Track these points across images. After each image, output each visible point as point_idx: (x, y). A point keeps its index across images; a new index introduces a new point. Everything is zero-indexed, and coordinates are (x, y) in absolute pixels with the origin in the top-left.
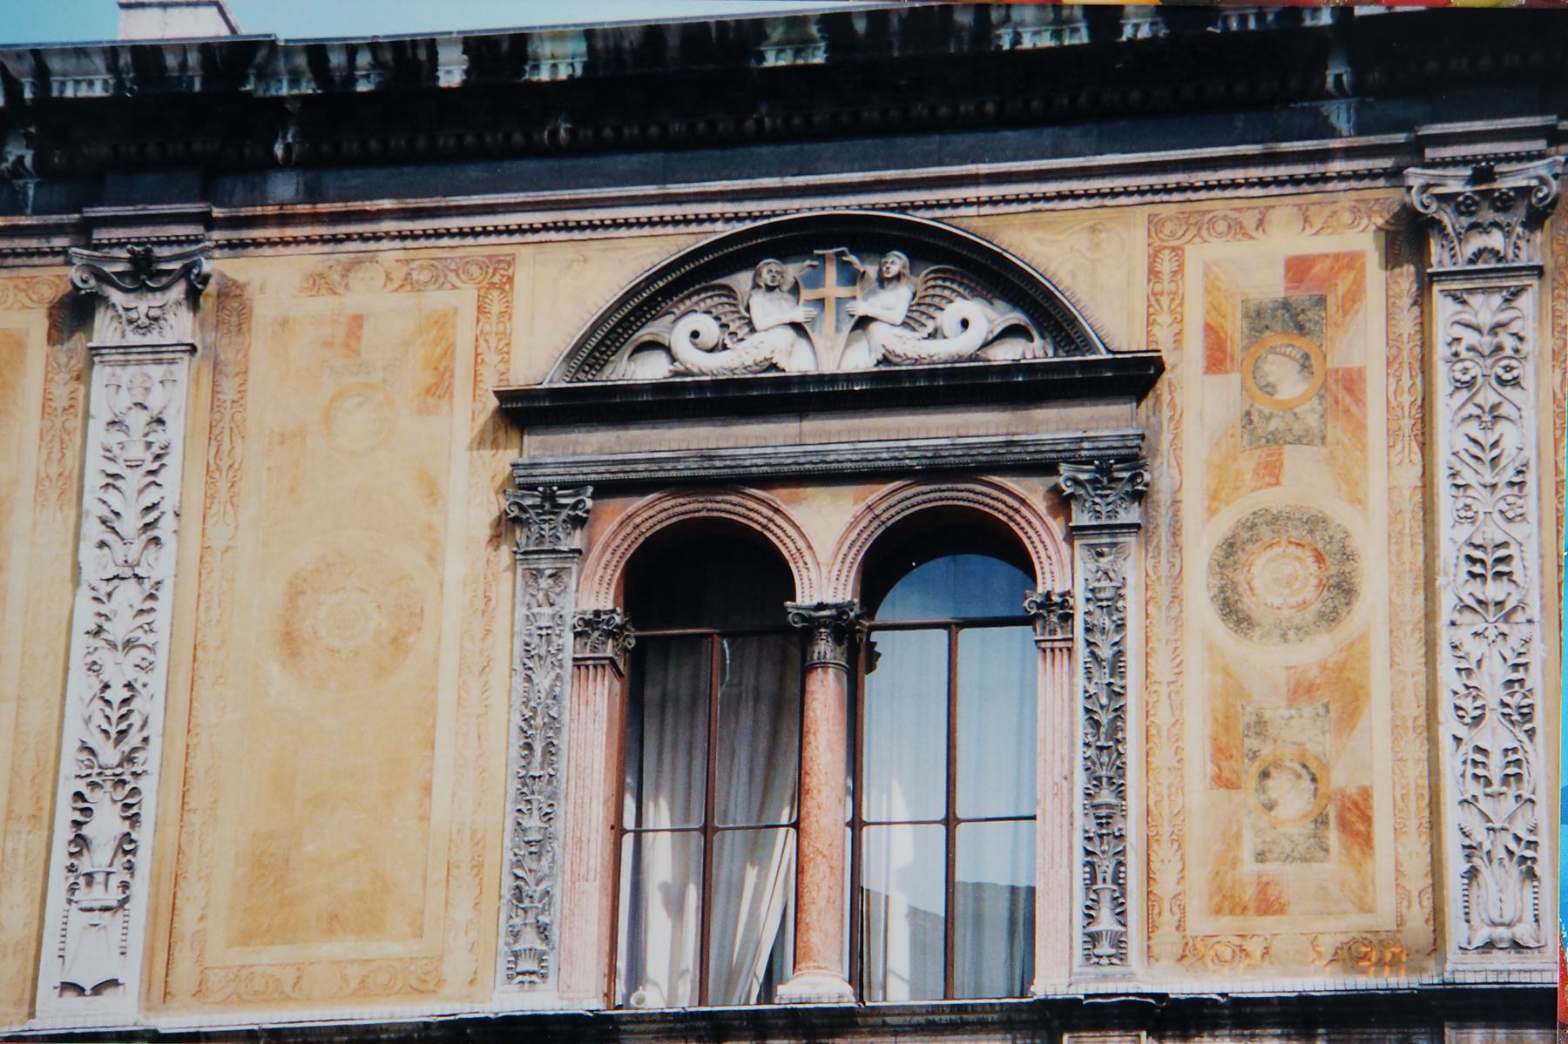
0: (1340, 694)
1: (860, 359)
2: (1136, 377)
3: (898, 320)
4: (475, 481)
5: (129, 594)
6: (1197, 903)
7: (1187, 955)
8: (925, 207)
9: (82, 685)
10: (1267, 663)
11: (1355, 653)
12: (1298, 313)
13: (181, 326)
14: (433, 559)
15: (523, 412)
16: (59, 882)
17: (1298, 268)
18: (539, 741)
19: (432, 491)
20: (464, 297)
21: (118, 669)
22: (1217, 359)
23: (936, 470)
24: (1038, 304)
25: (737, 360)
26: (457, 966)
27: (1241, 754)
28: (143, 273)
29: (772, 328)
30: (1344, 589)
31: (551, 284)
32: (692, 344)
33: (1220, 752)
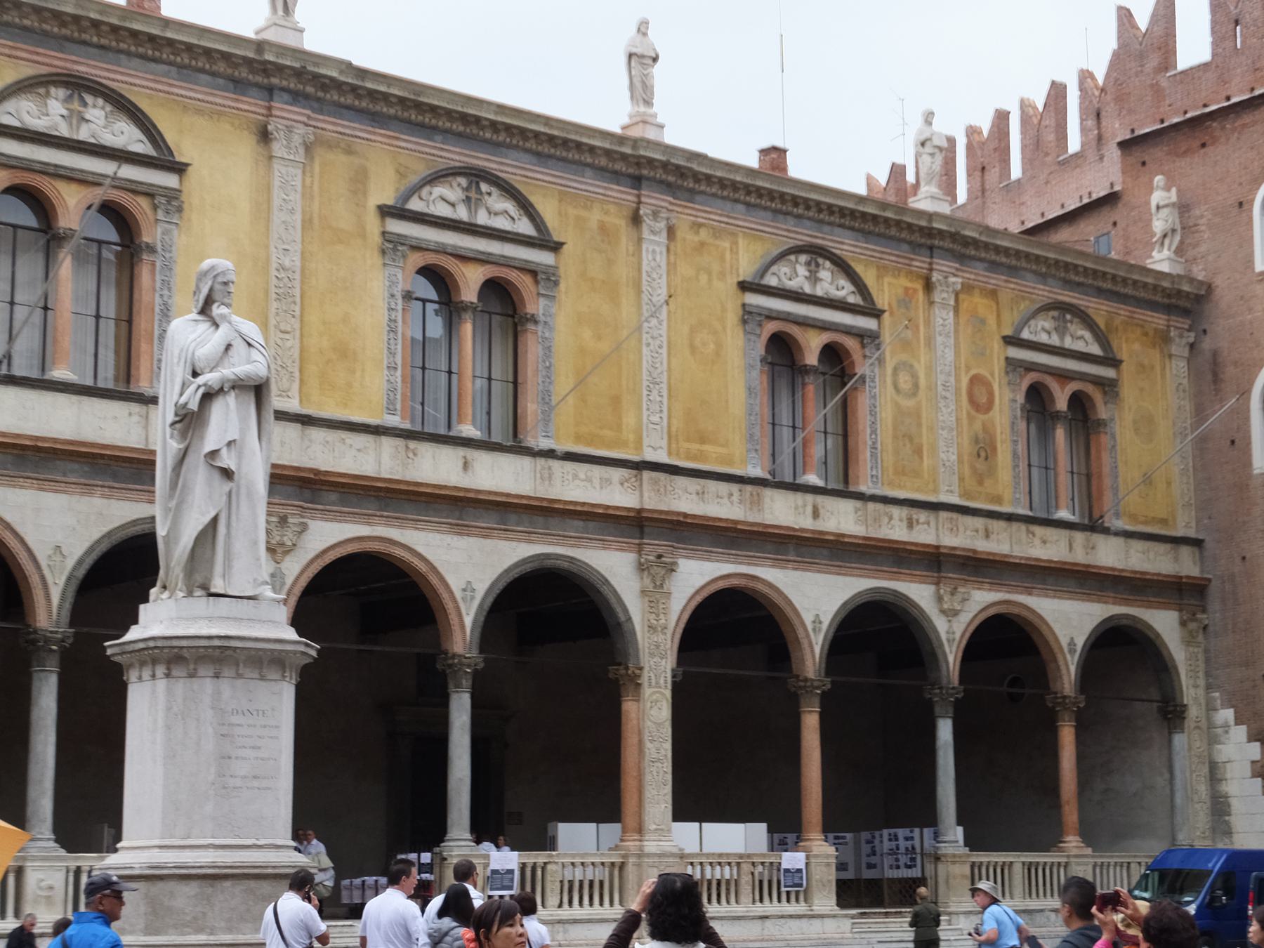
1: (819, 292)
6: (891, 470)
14: (724, 328)
15: (744, 286)
17: (907, 289)
19: (724, 310)
20: (727, 245)
24: (861, 287)
29: (794, 275)
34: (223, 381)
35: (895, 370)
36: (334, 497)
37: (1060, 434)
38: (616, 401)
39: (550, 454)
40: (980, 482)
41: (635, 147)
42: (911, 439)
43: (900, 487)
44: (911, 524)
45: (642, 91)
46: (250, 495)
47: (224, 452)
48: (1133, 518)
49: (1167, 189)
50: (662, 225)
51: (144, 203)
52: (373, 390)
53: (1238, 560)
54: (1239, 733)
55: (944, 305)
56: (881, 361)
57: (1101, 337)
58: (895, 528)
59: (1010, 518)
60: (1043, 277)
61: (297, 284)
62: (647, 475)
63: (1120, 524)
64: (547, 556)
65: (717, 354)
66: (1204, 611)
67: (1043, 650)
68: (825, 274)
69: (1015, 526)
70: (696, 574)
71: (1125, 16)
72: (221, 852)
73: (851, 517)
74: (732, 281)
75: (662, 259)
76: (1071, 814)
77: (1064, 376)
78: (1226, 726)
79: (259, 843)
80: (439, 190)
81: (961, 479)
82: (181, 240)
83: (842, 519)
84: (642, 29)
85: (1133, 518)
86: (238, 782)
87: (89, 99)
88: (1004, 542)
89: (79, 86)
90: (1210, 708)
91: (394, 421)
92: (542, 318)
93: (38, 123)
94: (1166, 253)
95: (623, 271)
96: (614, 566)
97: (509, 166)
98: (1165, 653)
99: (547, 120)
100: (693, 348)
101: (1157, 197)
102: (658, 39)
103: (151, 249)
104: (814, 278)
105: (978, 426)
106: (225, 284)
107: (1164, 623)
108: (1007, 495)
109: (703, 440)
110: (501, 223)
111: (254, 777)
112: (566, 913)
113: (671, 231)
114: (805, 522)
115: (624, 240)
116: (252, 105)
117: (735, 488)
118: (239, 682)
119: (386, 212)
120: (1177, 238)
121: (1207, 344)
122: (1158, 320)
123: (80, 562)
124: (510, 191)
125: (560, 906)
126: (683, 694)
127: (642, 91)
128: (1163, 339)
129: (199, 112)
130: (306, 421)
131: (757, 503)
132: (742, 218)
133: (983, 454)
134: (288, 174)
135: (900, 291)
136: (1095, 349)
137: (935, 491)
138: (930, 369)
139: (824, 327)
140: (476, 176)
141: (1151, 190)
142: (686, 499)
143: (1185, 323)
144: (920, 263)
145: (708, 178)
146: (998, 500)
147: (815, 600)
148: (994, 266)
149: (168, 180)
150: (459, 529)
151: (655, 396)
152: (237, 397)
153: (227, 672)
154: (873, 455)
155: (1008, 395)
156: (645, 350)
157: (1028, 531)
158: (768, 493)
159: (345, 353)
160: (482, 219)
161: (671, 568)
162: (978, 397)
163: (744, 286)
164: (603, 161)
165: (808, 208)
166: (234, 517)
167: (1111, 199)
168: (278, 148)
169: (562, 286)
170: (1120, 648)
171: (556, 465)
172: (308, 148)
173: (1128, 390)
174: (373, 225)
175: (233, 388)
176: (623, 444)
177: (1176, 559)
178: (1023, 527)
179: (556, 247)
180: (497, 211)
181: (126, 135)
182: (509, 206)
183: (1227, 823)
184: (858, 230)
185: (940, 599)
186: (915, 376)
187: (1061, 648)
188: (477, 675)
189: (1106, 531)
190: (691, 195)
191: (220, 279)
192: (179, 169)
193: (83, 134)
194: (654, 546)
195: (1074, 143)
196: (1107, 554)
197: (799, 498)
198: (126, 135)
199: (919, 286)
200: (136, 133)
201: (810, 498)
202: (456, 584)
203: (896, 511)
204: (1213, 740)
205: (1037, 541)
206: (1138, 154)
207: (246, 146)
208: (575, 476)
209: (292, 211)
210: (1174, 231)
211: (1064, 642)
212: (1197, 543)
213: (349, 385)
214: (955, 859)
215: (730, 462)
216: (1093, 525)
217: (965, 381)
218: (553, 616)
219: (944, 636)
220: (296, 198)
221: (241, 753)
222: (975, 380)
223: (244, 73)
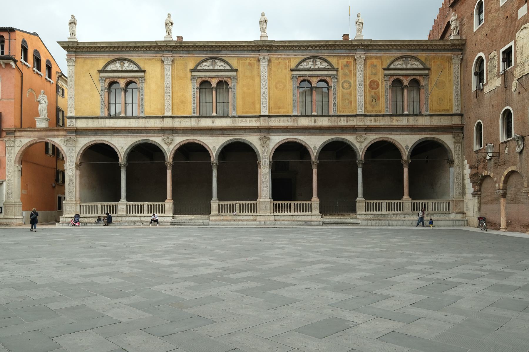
0: (350, 94)
2: (337, 70)
3: (319, 64)
4: (289, 75)
7: (340, 112)
10: (345, 91)
11: (351, 90)
12: (347, 65)
15: (292, 70)
17: (347, 62)
19: (286, 76)
20: (287, 61)
22: (342, 69)
25: (308, 67)
29: (310, 64)
30: (350, 86)
32: (303, 66)
33: (342, 97)
35: (343, 83)
36: (181, 132)
38: (254, 103)
39: (234, 117)
41: (254, 43)
42: (348, 100)
44: (347, 121)
45: (263, 30)
49: (455, 15)
50: (266, 60)
51: (137, 79)
52: (190, 109)
55: (360, 63)
56: (338, 81)
57: (421, 62)
58: (343, 122)
59: (383, 116)
60: (400, 50)
62: (261, 118)
63: (428, 113)
64: (235, 139)
65: (284, 87)
66: (463, 133)
69: (385, 118)
70: (277, 140)
73: (327, 121)
74: (288, 69)
75: (266, 68)
76: (406, 190)
77: (406, 76)
80: (204, 64)
82: (145, 86)
83: (324, 122)
84: (263, 14)
85: (435, 111)
88: (381, 122)
89: (122, 60)
91: (195, 115)
93: (115, 69)
95: (255, 73)
96: (254, 140)
98: (446, 146)
99: (229, 42)
100: (276, 88)
104: (315, 64)
105: (373, 93)
107: (447, 139)
109: (279, 108)
113: (269, 61)
115: (256, 65)
116: (159, 55)
117: (289, 118)
119: (192, 71)
122: (449, 54)
123: (127, 150)
127: (263, 30)
128: (449, 60)
129: (148, 59)
130: (173, 117)
131: (296, 121)
132: (291, 53)
133: (374, 100)
135: (345, 63)
136: (421, 66)
137: (356, 112)
138: (355, 81)
139: (318, 76)
140: (214, 59)
142: (274, 123)
143: (460, 53)
144: (351, 54)
145: (278, 46)
146: (380, 111)
148: (380, 50)
149: (142, 74)
150: (211, 136)
151: (264, 100)
154: (334, 106)
155: (384, 83)
156: (261, 90)
157: (391, 118)
158: (300, 118)
159: (183, 102)
160: (216, 68)
161: (269, 139)
162: (373, 85)
163: (292, 70)
164: (249, 48)
165: (320, 47)
168: (165, 63)
169: (239, 79)
171: (236, 119)
172: (173, 61)
174: (189, 74)
176: (256, 112)
177: (452, 120)
178: (389, 118)
179: (236, 71)
180: (220, 65)
181: (132, 67)
182: (223, 64)
184: (330, 50)
187: (403, 148)
189: (422, 115)
190: (276, 51)
192: (144, 71)
193: (124, 69)
194: (263, 135)
196: (423, 121)
197: (310, 118)
198: (132, 67)
199: (352, 60)
200: (135, 66)
201: (313, 118)
203: (342, 118)
205: (394, 121)
207: (159, 64)
208: (242, 121)
210: (457, 27)
211: (404, 146)
212: (461, 115)
213: (184, 109)
219: (358, 148)
223: (157, 49)
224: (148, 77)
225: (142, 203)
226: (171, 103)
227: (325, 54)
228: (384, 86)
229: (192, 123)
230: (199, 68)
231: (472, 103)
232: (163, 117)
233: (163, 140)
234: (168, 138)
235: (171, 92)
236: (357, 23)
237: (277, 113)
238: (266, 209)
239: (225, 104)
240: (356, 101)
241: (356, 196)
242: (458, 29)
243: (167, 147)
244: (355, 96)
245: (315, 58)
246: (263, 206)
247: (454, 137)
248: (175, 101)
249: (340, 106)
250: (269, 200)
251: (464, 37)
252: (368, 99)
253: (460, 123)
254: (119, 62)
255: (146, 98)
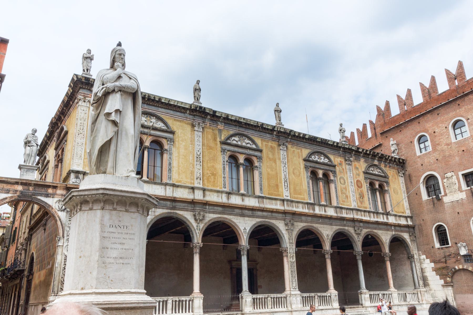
0: (345, 188)
2: (334, 166)
3: (323, 160)
5: (285, 168)
7: (341, 204)
8: (325, 152)
9: (283, 174)
13: (285, 149)
16: (284, 188)
17: (340, 161)
18: (308, 184)
20: (300, 151)
21: (285, 173)
23: (326, 170)
24: (330, 160)
26: (306, 198)
27: (342, 193)
28: (283, 144)
29: (315, 158)
30: (345, 182)
31: (305, 152)
32: (313, 158)
34: (115, 87)
35: (340, 178)
37: (378, 193)
38: (277, 186)
40: (362, 204)
43: (343, 205)
46: (127, 134)
47: (113, 114)
48: (396, 212)
51: (164, 140)
53: (422, 221)
54: (428, 261)
61: (201, 158)
67: (380, 243)
68: (323, 158)
71: (378, 109)
72: (99, 296)
78: (424, 259)
79: (122, 291)
80: (233, 138)
81: (357, 203)
86: (112, 260)
87: (152, 117)
90: (419, 255)
91: (226, 190)
92: (258, 166)
94: (395, 154)
95: (277, 156)
97: (249, 133)
100: (294, 173)
101: (392, 142)
102: (281, 107)
103: (166, 150)
105: (359, 191)
106: (120, 54)
107: (406, 236)
108: (368, 206)
110: (248, 145)
111: (121, 258)
112: (273, 310)
114: (323, 213)
118: (114, 212)
120: (397, 151)
121: (407, 173)
124: (250, 139)
125: (272, 308)
126: (298, 254)
127: (279, 119)
134: (198, 135)
135: (339, 162)
141: (389, 141)
146: (366, 208)
147: (327, 233)
149: (170, 136)
152: (121, 95)
153: (107, 207)
156: (283, 174)
159: (214, 175)
160: (244, 144)
166: (119, 144)
167: (380, 145)
168: (196, 128)
169: (263, 159)
170: (397, 242)
172: (203, 128)
173: (391, 184)
175: (120, 91)
181: (160, 125)
183: (428, 283)
185: (355, 231)
186: (344, 180)
188: (248, 251)
189: (391, 215)
191: (118, 52)
192: (173, 133)
195: (370, 135)
196: (392, 220)
198: (160, 125)
202: (242, 228)
204: (421, 263)
206: (385, 135)
207: (189, 128)
209: (200, 142)
212: (411, 217)
213: (214, 181)
214: (365, 294)
215: (305, 200)
216: (387, 214)
217: (355, 181)
218: (265, 237)
220: (201, 139)
221: (114, 246)
222: (358, 181)
224: (177, 140)
225: (165, 298)
226: (201, 173)
227: (326, 150)
228: (365, 186)
229: (223, 199)
230: (229, 141)
231: (425, 209)
232: (193, 189)
233: (195, 215)
234: (199, 214)
235: (201, 160)
236: (341, 130)
237: (296, 199)
238: (297, 304)
239: (250, 183)
240: (350, 196)
241: (359, 287)
242: (397, 151)
243: (197, 224)
244: (349, 192)
245: (320, 153)
246: (293, 299)
247: (410, 236)
248: (206, 172)
249: (340, 199)
250: (299, 292)
251: (403, 158)
252: (358, 196)
253: (412, 224)
254: (145, 116)
255: (175, 164)
